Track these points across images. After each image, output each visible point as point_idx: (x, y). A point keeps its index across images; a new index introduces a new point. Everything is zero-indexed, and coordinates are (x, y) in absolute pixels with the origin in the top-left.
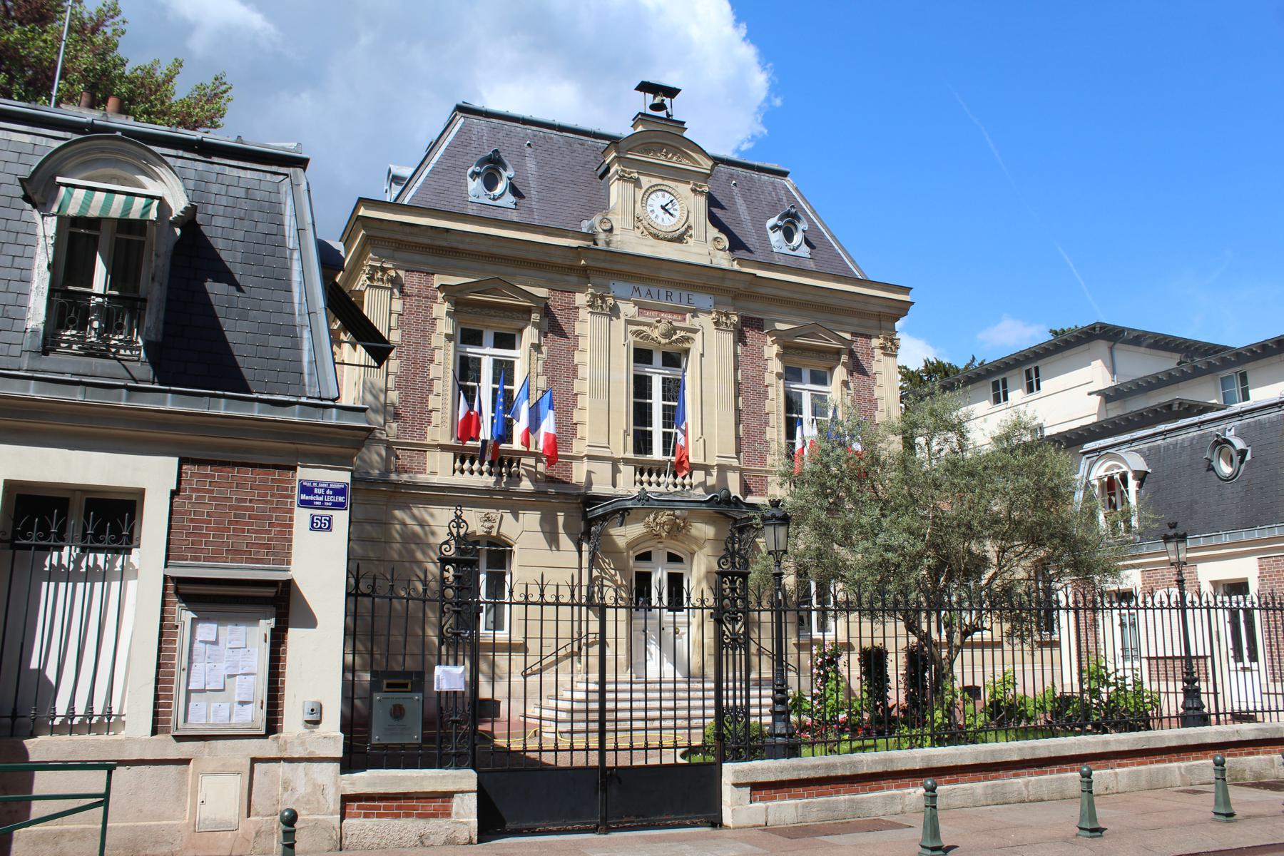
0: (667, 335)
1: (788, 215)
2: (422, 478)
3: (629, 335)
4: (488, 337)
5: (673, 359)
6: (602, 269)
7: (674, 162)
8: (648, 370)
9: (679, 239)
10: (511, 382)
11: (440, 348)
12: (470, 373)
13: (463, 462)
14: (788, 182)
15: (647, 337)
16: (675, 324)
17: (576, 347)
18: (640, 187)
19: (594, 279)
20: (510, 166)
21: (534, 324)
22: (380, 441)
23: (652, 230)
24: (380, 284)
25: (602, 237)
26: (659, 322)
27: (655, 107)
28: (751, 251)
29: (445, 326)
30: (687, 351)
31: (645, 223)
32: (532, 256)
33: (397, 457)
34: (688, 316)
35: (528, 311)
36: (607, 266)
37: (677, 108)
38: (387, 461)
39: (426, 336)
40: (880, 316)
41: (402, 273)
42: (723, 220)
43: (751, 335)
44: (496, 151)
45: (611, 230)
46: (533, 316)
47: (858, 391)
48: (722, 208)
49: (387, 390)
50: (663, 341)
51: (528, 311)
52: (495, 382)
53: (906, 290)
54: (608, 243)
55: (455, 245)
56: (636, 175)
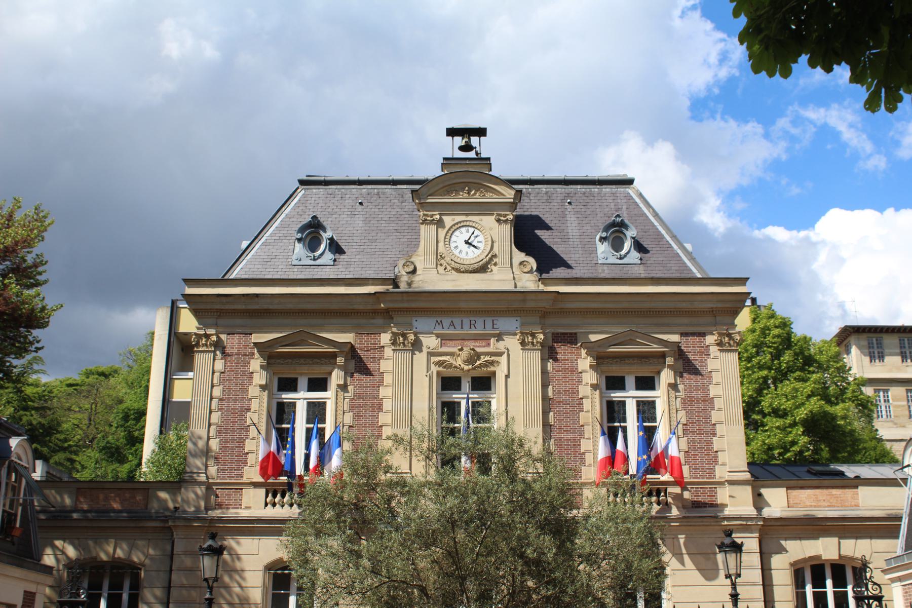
0: (470, 360)
1: (613, 224)
2: (231, 513)
3: (433, 366)
4: (303, 382)
5: (483, 383)
6: (398, 308)
7: (478, 198)
8: (456, 396)
9: (483, 269)
10: (323, 421)
11: (256, 398)
12: (285, 416)
13: (274, 496)
14: (630, 191)
15: (450, 366)
16: (478, 350)
17: (381, 383)
18: (444, 227)
19: (398, 319)
20: (328, 227)
21: (340, 367)
22: (200, 484)
23: (457, 266)
24: (204, 349)
25: (404, 279)
26: (461, 350)
27: (462, 148)
28: (569, 267)
29: (260, 378)
30: (494, 373)
31: (448, 259)
32: (335, 306)
33: (217, 496)
34: (493, 340)
35: (334, 356)
36: (406, 305)
37: (484, 146)
38: (207, 499)
39: (244, 388)
40: (713, 312)
41: (223, 337)
42: (547, 241)
43: (562, 351)
44: (314, 217)
45: (414, 272)
46: (338, 359)
47: (688, 391)
48: (548, 228)
49: (209, 438)
50: (466, 368)
51: (334, 356)
52: (308, 422)
53: (743, 281)
54: (409, 284)
55: (265, 307)
56: (438, 217)
